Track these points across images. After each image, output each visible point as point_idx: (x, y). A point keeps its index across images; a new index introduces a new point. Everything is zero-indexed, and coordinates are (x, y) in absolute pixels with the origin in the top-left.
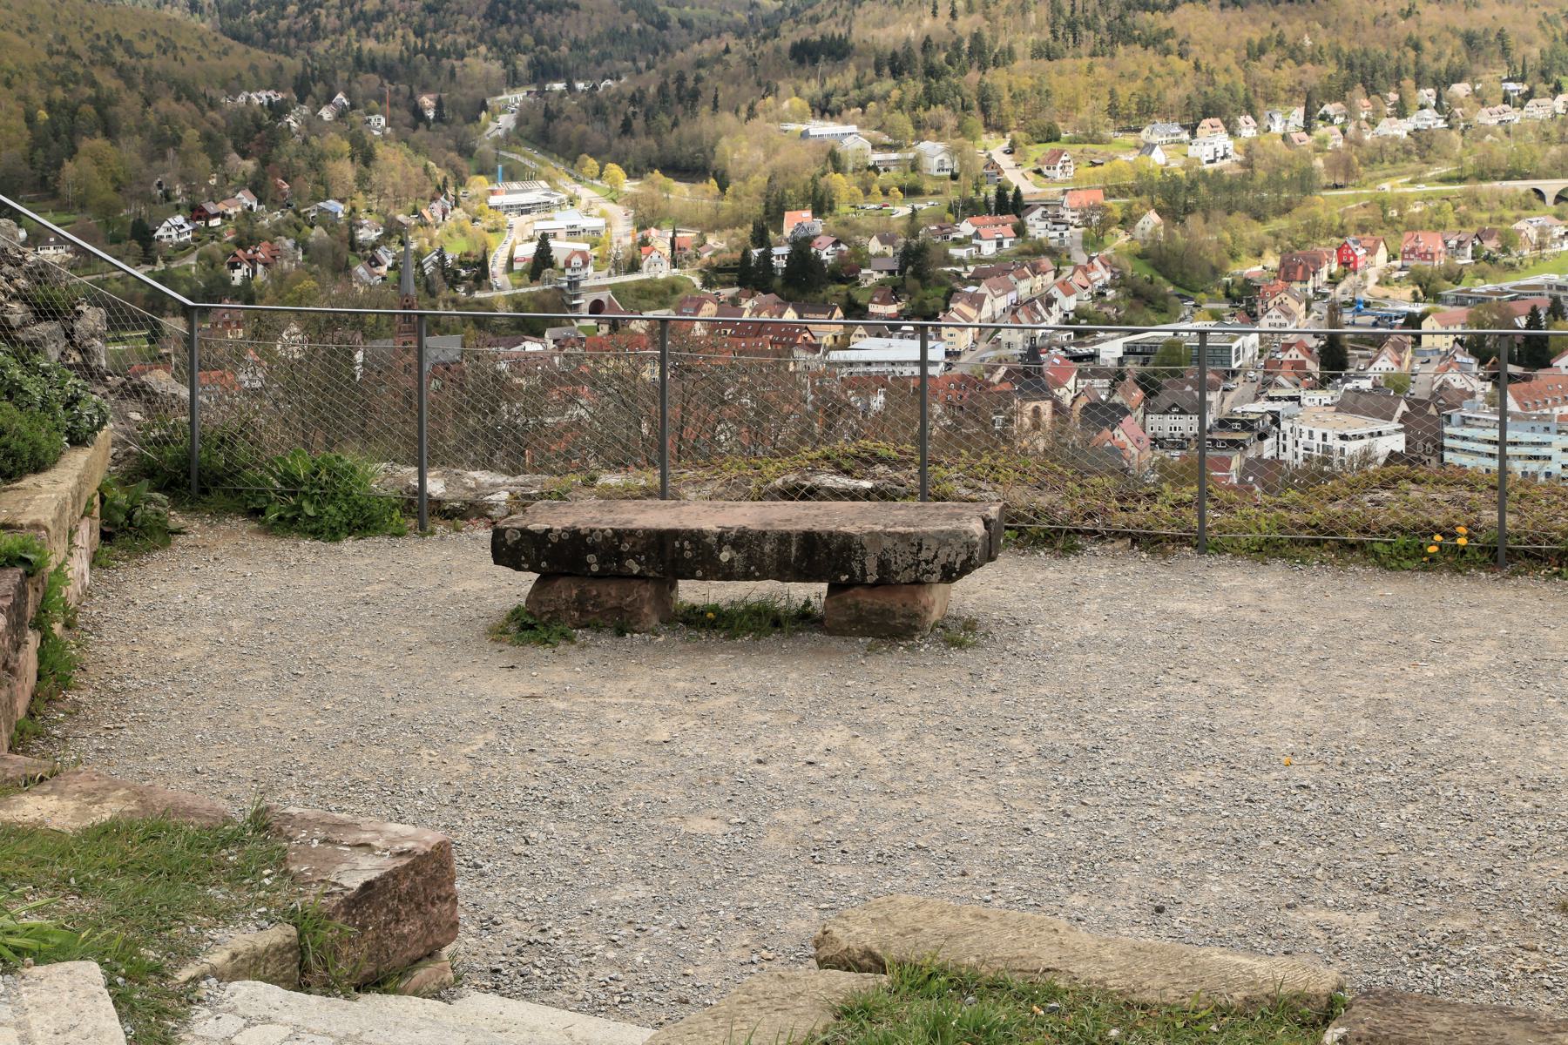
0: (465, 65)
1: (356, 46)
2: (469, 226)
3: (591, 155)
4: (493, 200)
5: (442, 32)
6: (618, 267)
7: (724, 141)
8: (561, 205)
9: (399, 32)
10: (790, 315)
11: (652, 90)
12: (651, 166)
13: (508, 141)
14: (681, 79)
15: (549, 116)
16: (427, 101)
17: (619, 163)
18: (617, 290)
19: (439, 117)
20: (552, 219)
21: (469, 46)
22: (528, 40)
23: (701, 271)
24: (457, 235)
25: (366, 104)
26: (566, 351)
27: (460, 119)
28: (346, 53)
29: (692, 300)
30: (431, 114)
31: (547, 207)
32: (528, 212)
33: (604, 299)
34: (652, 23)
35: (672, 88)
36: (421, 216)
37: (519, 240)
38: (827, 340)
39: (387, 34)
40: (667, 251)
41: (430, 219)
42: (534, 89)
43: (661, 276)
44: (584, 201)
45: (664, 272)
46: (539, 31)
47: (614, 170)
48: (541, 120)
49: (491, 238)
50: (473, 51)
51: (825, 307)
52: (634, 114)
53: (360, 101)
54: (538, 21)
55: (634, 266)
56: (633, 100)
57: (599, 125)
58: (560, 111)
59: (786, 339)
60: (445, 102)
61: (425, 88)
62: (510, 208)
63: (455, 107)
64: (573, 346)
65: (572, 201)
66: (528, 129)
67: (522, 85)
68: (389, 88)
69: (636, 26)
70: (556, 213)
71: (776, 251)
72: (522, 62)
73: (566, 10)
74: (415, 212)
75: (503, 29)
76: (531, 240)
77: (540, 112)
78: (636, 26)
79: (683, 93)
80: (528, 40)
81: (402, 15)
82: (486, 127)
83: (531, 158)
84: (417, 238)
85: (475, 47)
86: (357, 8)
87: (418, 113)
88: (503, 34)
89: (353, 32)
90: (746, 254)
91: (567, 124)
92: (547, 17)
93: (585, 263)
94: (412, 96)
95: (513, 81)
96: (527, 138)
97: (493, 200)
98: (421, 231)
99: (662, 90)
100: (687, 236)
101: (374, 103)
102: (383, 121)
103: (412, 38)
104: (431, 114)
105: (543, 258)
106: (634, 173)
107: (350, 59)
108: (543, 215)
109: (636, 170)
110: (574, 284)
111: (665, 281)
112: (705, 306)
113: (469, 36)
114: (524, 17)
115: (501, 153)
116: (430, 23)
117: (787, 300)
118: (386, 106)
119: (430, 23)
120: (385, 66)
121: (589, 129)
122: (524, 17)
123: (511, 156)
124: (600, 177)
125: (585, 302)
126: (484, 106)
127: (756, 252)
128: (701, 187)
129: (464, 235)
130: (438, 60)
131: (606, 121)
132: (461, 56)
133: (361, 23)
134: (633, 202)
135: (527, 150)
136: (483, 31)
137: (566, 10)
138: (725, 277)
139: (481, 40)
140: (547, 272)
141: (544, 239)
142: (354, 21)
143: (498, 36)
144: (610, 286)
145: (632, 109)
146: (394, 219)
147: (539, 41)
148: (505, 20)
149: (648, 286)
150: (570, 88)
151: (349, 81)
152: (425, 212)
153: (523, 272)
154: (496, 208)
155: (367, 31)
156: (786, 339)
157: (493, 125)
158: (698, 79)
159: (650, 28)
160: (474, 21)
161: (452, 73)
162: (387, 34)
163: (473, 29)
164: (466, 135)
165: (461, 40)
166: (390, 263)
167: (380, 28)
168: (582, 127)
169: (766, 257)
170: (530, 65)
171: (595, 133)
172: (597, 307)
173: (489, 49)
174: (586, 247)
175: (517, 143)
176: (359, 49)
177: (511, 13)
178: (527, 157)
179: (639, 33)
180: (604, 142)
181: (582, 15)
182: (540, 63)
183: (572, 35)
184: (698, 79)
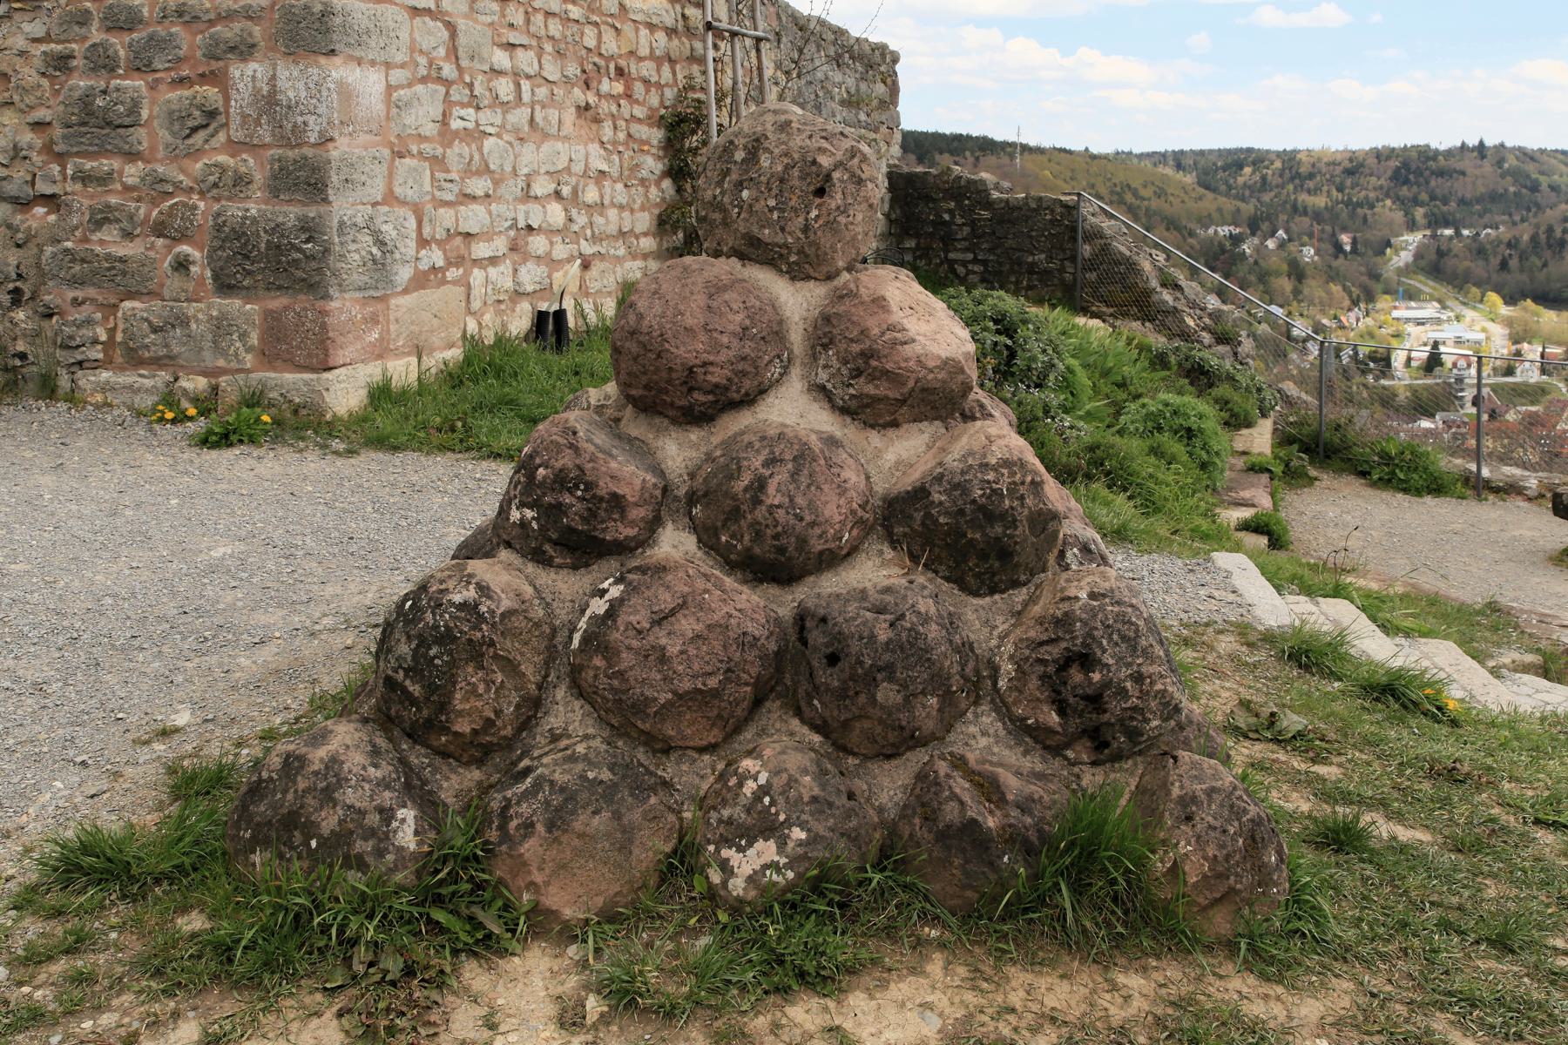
0: (1374, 214)
1: (1293, 197)
3: (1474, 285)
4: (1396, 314)
5: (1357, 189)
8: (1449, 320)
9: (1325, 188)
11: (1526, 237)
12: (1524, 296)
13: (1406, 271)
14: (1550, 230)
15: (1440, 253)
16: (1345, 239)
17: (1498, 292)
19: (1354, 250)
21: (1378, 200)
22: (1424, 197)
25: (1300, 239)
27: (1370, 252)
28: (1286, 202)
30: (1348, 248)
31: (1438, 321)
32: (1423, 324)
34: (1526, 187)
35: (1543, 237)
36: (1340, 321)
39: (1316, 190)
42: (1428, 233)
43: (1532, 381)
44: (1468, 319)
46: (1433, 191)
47: (1493, 297)
48: (1434, 257)
49: (1394, 343)
50: (1381, 204)
52: (1510, 255)
53: (1295, 236)
54: (1433, 183)
56: (1509, 245)
57: (1481, 263)
58: (1450, 250)
60: (1359, 240)
61: (1344, 229)
62: (1408, 320)
63: (1367, 243)
66: (1423, 263)
67: (1418, 229)
68: (1317, 228)
69: (1512, 189)
72: (1419, 213)
73: (1455, 175)
74: (1335, 318)
75: (1405, 188)
76: (1425, 345)
77: (1434, 251)
78: (1512, 189)
79: (1552, 241)
80: (1424, 197)
81: (1328, 176)
82: (1390, 259)
83: (1426, 285)
85: (1382, 200)
87: (1338, 247)
88: (1404, 191)
89: (1291, 187)
91: (1454, 261)
92: (1440, 180)
94: (1334, 235)
95: (1412, 226)
96: (1422, 269)
97: (1396, 314)
99: (1534, 239)
101: (1305, 238)
102: (1312, 252)
103: (1334, 193)
104: (1348, 248)
105: (1434, 361)
106: (1510, 300)
107: (1288, 206)
108: (1436, 327)
113: (1378, 193)
114: (1421, 180)
115: (1403, 279)
118: (1315, 241)
119: (1348, 182)
120: (1314, 212)
121: (1472, 265)
122: (1421, 180)
123: (1411, 282)
124: (1481, 301)
126: (1388, 244)
130: (1354, 209)
131: (1487, 260)
132: (1372, 207)
133: (1297, 181)
134: (1509, 322)
136: (1389, 189)
137: (1455, 175)
139: (1387, 196)
141: (1436, 345)
142: (1292, 179)
143: (1401, 193)
146: (1319, 322)
147: (1433, 198)
148: (1406, 182)
150: (1458, 234)
151: (1287, 222)
152: (1343, 318)
153: (1418, 368)
154: (1398, 319)
155: (1302, 186)
157: (1395, 259)
159: (1524, 191)
160: (1382, 182)
161: (1365, 219)
162: (1316, 190)
163: (1381, 187)
165: (1372, 195)
167: (1310, 184)
168: (1467, 263)
170: (1426, 216)
171: (1478, 268)
173: (1394, 203)
175: (1415, 273)
176: (1296, 199)
177: (1411, 177)
180: (1486, 275)
182: (1433, 214)
183: (1460, 195)
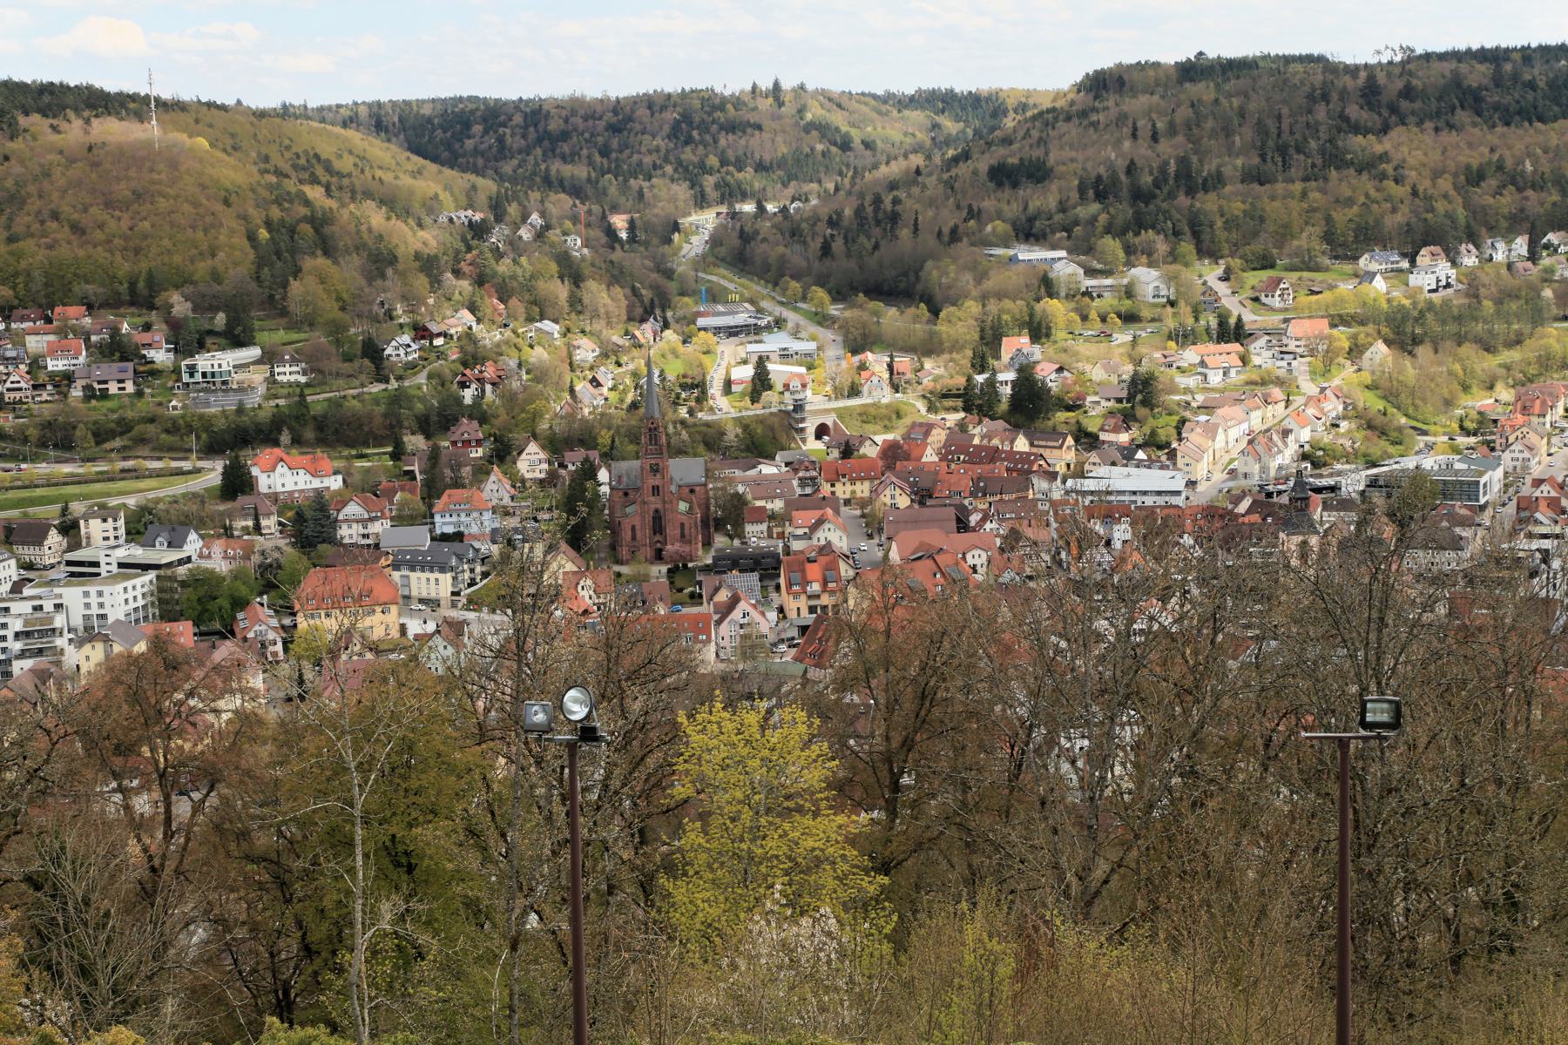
0: (652, 186)
1: (543, 167)
2: (681, 348)
3: (792, 277)
4: (701, 322)
5: (627, 152)
6: (838, 393)
7: (929, 264)
8: (768, 328)
9: (585, 152)
10: (1022, 444)
11: (848, 212)
12: (854, 289)
13: (703, 263)
14: (877, 200)
15: (746, 237)
16: (619, 222)
17: (822, 286)
18: (841, 413)
19: (632, 239)
20: (760, 342)
21: (655, 167)
22: (713, 161)
23: (924, 397)
24: (670, 356)
25: (561, 225)
26: (801, 474)
27: (655, 241)
28: (534, 173)
29: (921, 425)
30: (624, 235)
31: (757, 330)
32: (736, 334)
33: (830, 423)
34: (835, 144)
35: (869, 210)
36: (634, 337)
37: (733, 362)
38: (1060, 468)
39: (573, 154)
40: (886, 375)
41: (643, 341)
42: (724, 209)
43: (885, 401)
44: (790, 325)
45: (887, 397)
46: (723, 152)
47: (820, 293)
48: (737, 242)
49: (706, 359)
50: (659, 172)
51: (1055, 434)
52: (832, 236)
53: (554, 221)
54: (723, 142)
55: (854, 391)
56: (832, 223)
57: (798, 248)
58: (757, 232)
59: (1022, 469)
60: (638, 223)
61: (615, 209)
62: (717, 330)
63: (648, 227)
64: (807, 469)
65: (779, 323)
66: (722, 251)
67: (709, 206)
68: (582, 209)
69: (819, 147)
70: (765, 336)
71: (1001, 377)
72: (709, 181)
73: (749, 130)
74: (627, 333)
75: (688, 149)
76: (745, 362)
77: (735, 234)
78: (819, 147)
79: (881, 216)
80: (713, 161)
81: (587, 135)
82: (680, 248)
83: (731, 281)
84: (633, 359)
85: (661, 167)
86: (541, 127)
87: (611, 232)
88: (688, 154)
89: (539, 151)
90: (969, 379)
91: (764, 246)
92: (731, 137)
93: (804, 386)
94: (604, 217)
95: (701, 202)
96: (723, 260)
97: (701, 322)
98: (635, 352)
99: (859, 212)
100: (904, 362)
101: (568, 224)
102: (579, 242)
103: (597, 158)
104: (624, 235)
105: (762, 381)
106: (838, 296)
107: (538, 179)
108: (752, 338)
109: (838, 293)
110: (799, 407)
111: (887, 406)
112: (934, 432)
113: (654, 156)
114: (708, 137)
115: (701, 275)
116: (615, 143)
117: (1017, 427)
118: (581, 227)
119: (615, 143)
120: (574, 186)
121: (788, 251)
122: (708, 137)
123: (714, 278)
124: (804, 299)
125: (810, 426)
126: (676, 227)
127: (980, 378)
128: (912, 311)
129: (677, 357)
130: (626, 181)
131: (804, 243)
132: (649, 178)
133: (546, 143)
134: (845, 328)
135: (722, 271)
136: (668, 151)
137: (749, 130)
138: (949, 403)
139: (666, 160)
140: (767, 396)
141: (761, 362)
142: (539, 141)
143: (683, 157)
144: (834, 410)
145: (829, 231)
146: (609, 341)
147: (724, 162)
148: (689, 141)
149: (872, 411)
150: (761, 209)
151: (542, 201)
152: (637, 333)
153: (743, 394)
154: (705, 329)
155: (553, 151)
156: (1022, 469)
157: (686, 247)
158: (896, 201)
159: (834, 149)
160: (658, 142)
161: (641, 194)
162: (573, 154)
163: (658, 150)
164: (663, 255)
165: (647, 160)
166: (610, 384)
167: (566, 148)
168: (781, 249)
169: (991, 384)
170: (717, 186)
171: (796, 256)
172: (821, 431)
173: (676, 170)
174: (803, 370)
175: (715, 265)
176: (547, 170)
177: (695, 133)
178: (722, 278)
179: (823, 154)
180: (804, 264)
181: (766, 136)
182: (727, 185)
183: (757, 156)
184: (896, 201)
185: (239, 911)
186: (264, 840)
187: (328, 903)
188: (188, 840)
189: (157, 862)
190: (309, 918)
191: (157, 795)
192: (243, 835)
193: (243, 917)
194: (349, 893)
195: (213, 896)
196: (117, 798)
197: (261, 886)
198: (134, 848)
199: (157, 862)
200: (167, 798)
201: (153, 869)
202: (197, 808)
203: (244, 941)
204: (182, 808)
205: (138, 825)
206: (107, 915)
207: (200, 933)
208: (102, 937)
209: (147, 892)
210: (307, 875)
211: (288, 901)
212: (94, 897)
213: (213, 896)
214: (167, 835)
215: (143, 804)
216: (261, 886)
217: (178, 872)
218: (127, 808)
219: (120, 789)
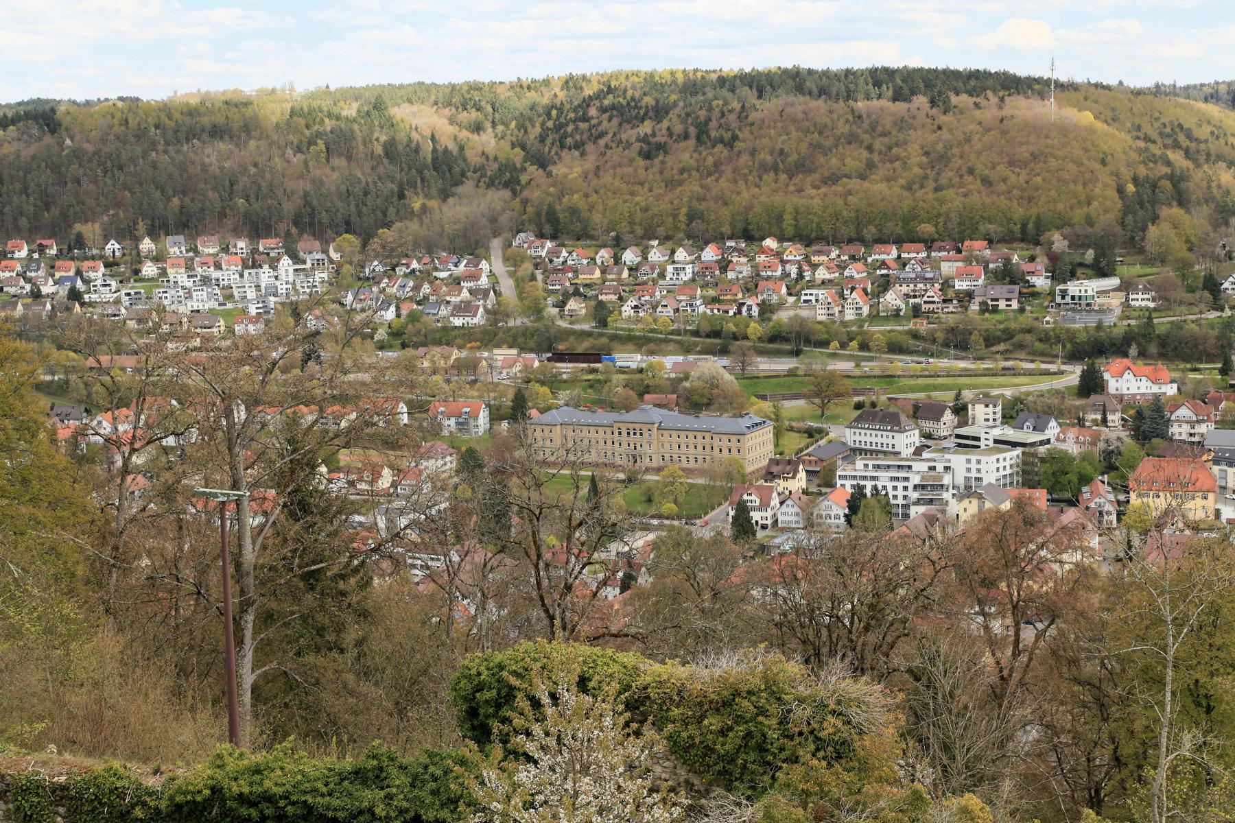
185: (1065, 721)
186: (1090, 669)
187: (1138, 726)
188: (1030, 659)
189: (1005, 673)
190: (1122, 735)
191: (1009, 621)
192: (1074, 662)
193: (1069, 726)
194: (1157, 720)
195: (1046, 706)
196: (980, 619)
197: (1084, 705)
198: (987, 659)
199: (1005, 673)
200: (1017, 625)
201: (1002, 678)
202: (1040, 635)
203: (1068, 745)
204: (1028, 634)
205: (993, 643)
206: (966, 707)
207: (1034, 733)
208: (962, 723)
209: (996, 696)
210: (1124, 701)
211: (1106, 720)
212: (958, 692)
213: (1046, 706)
214: (1016, 653)
215: (997, 626)
216: (1084, 705)
217: (1022, 683)
218: (987, 628)
219: (982, 613)
